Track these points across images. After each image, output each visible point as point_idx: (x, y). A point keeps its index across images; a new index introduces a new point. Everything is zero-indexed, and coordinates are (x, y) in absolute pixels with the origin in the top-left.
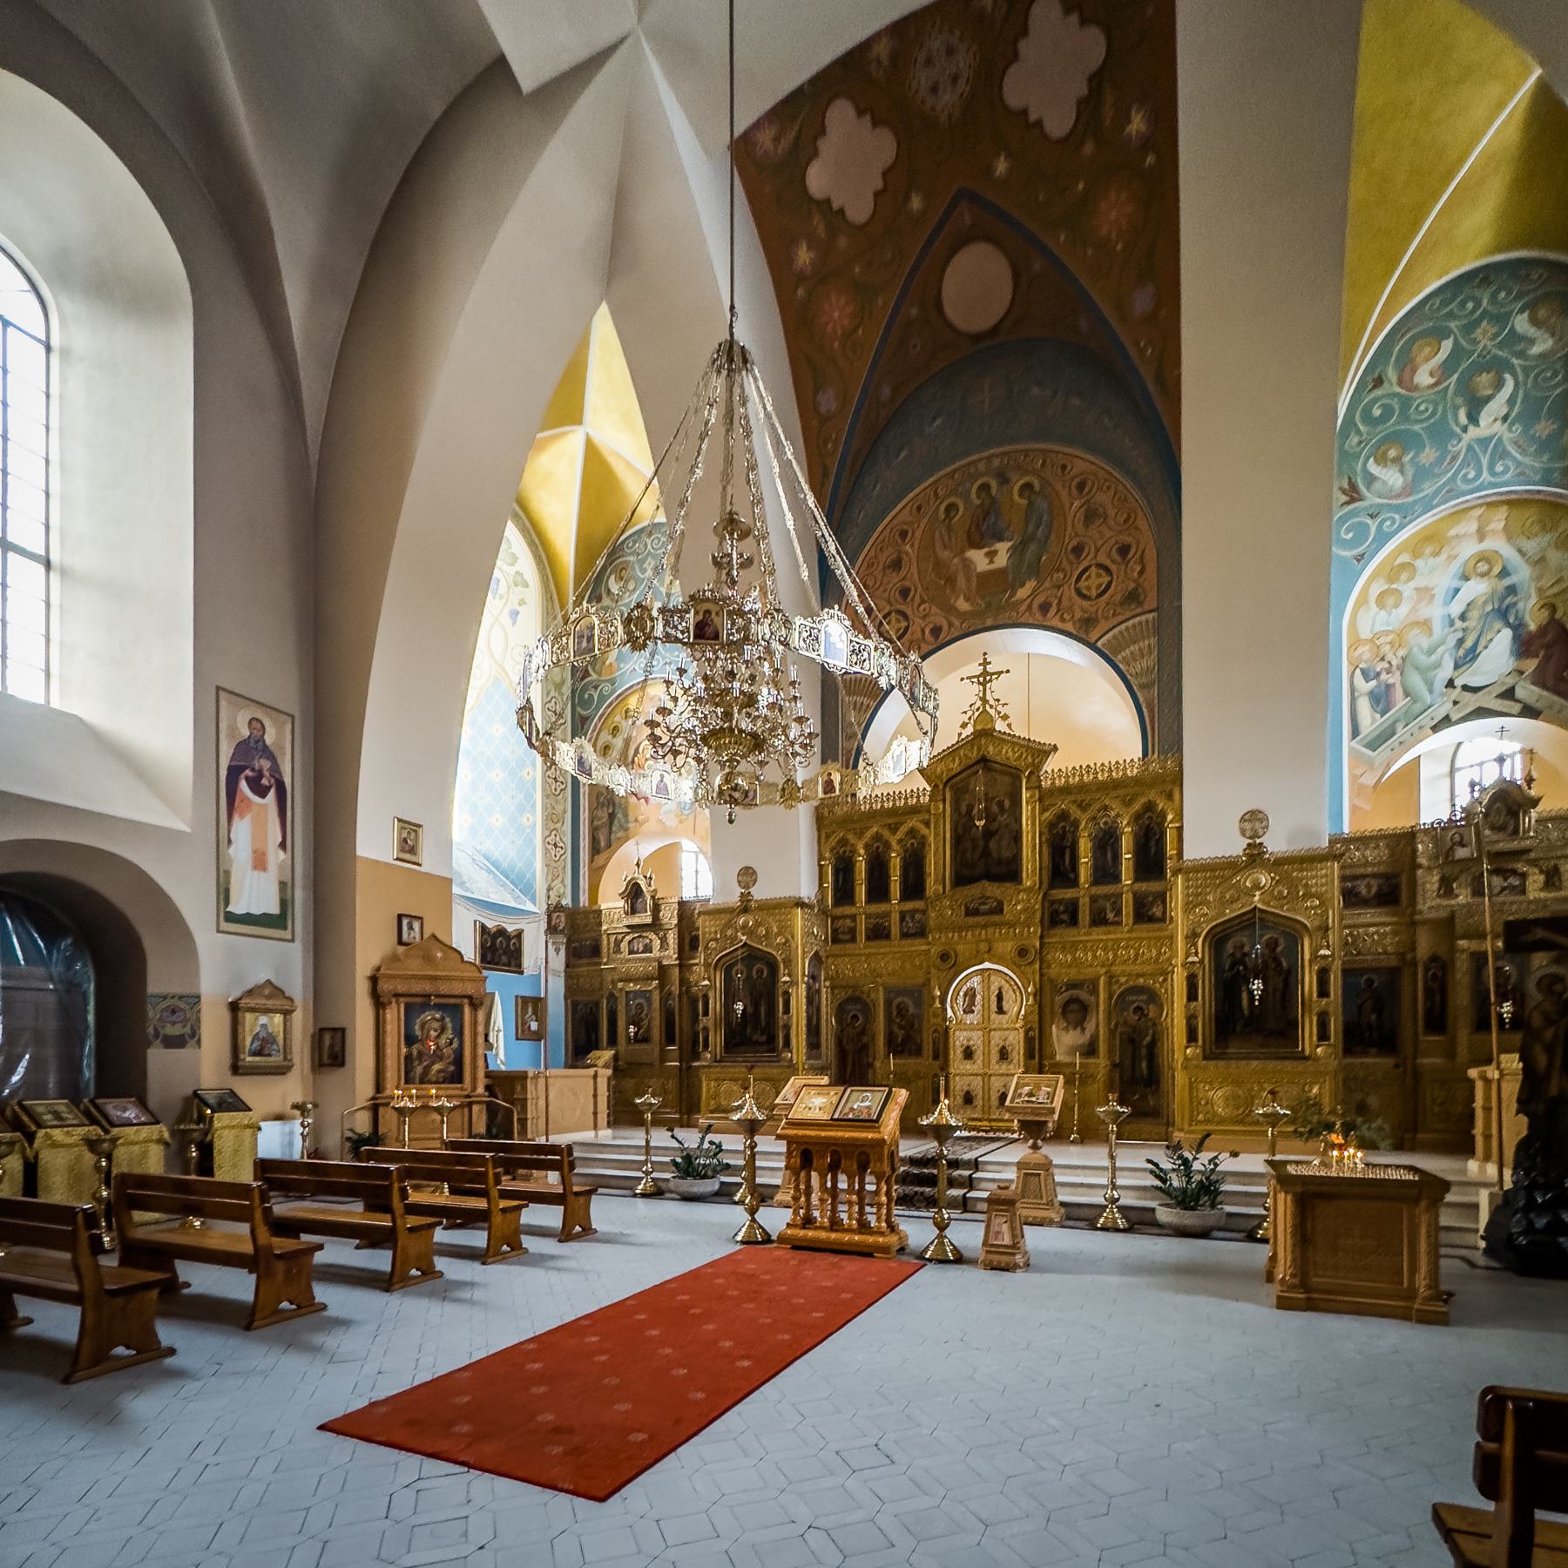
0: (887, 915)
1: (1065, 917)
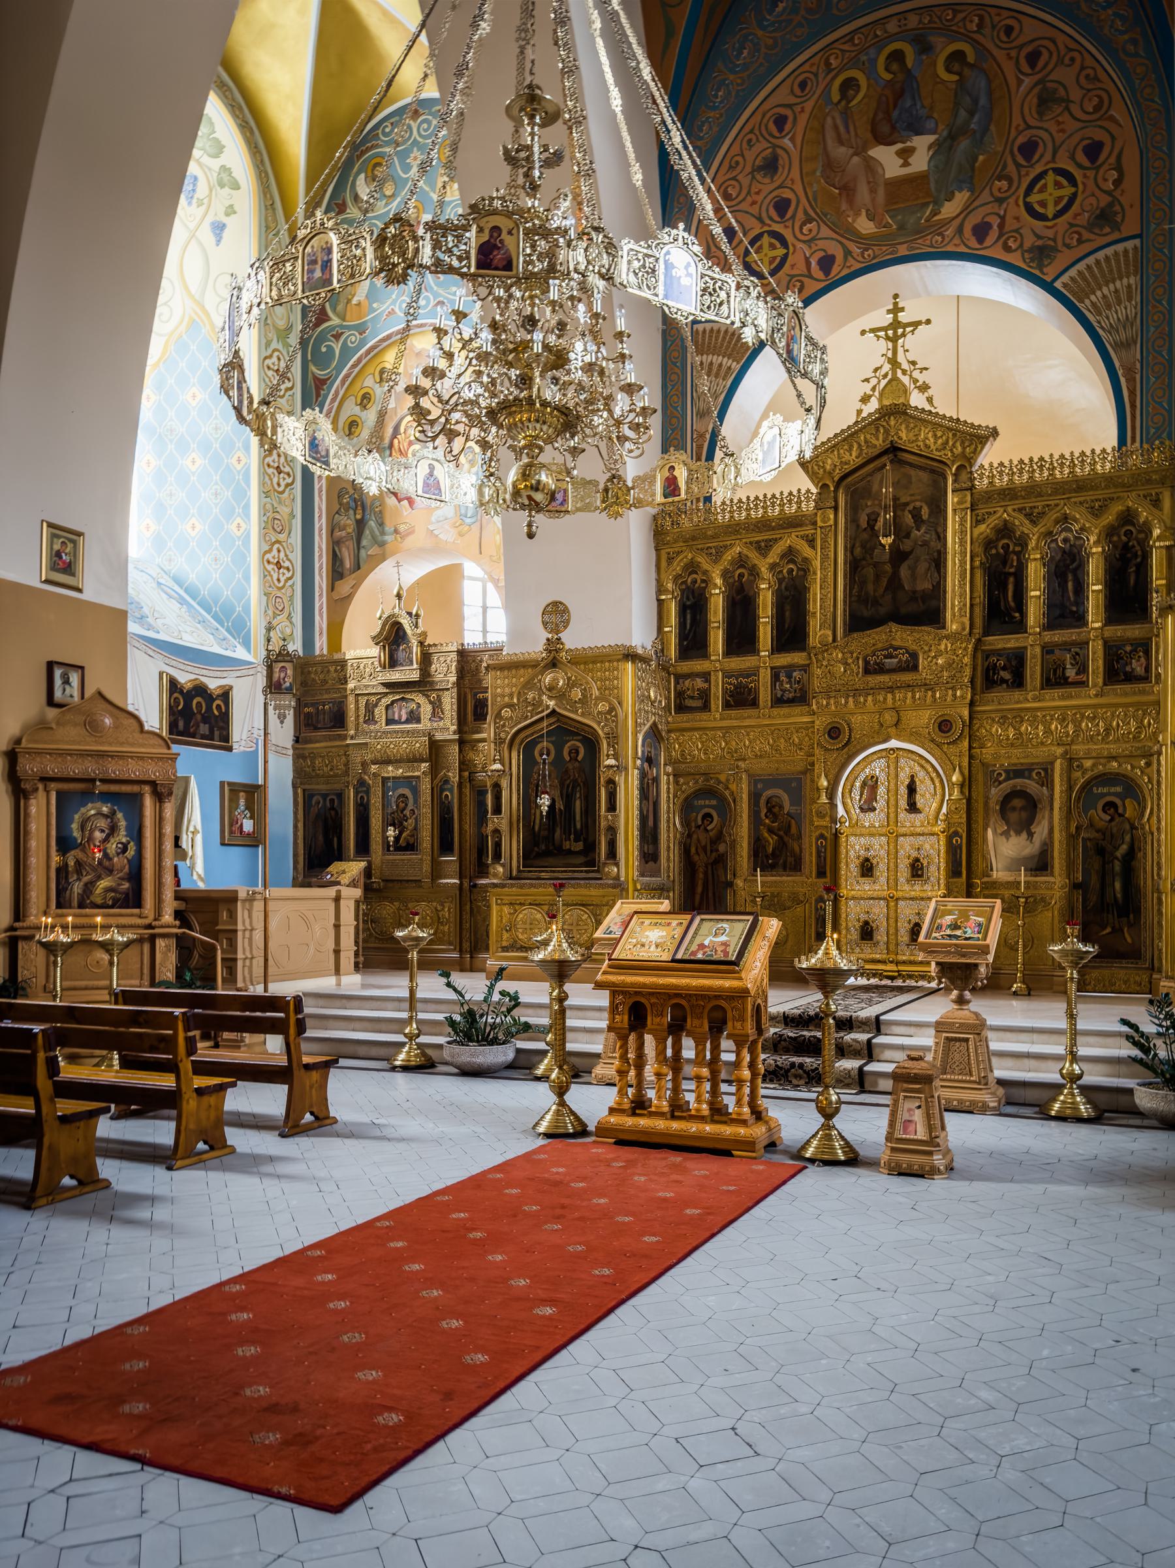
0: (753, 673)
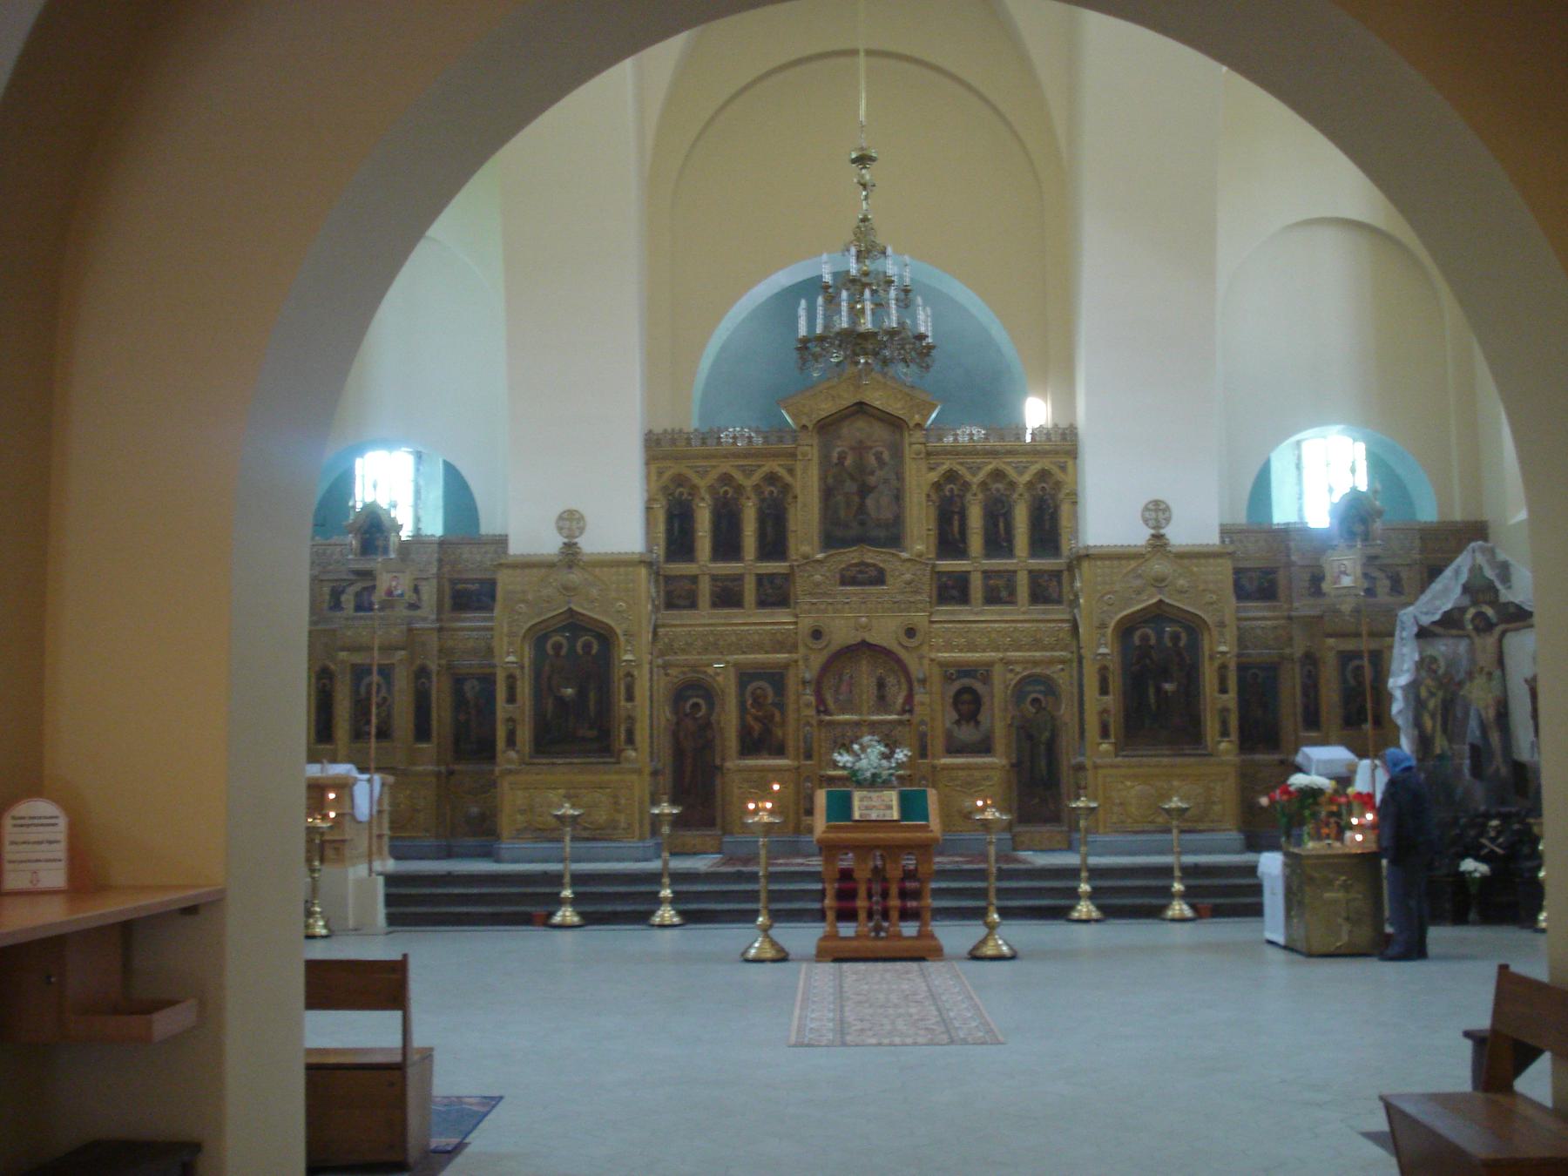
0: (739, 578)
1: (955, 593)
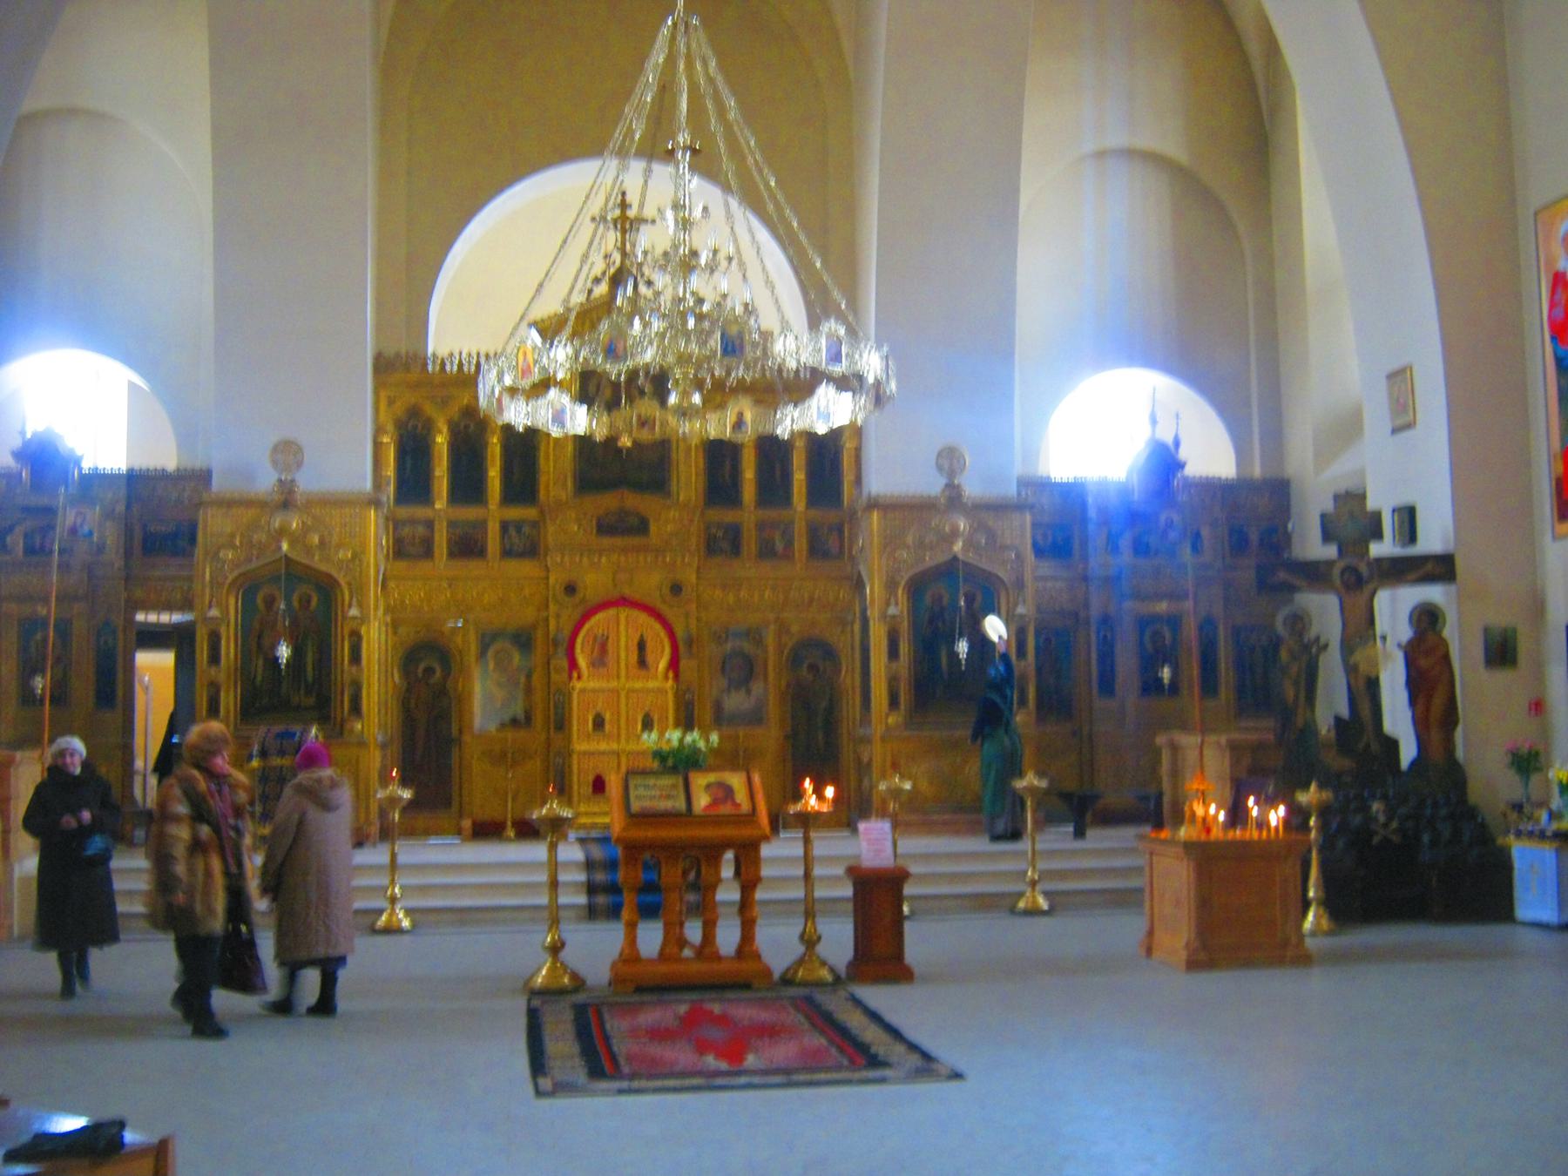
1: (725, 545)
